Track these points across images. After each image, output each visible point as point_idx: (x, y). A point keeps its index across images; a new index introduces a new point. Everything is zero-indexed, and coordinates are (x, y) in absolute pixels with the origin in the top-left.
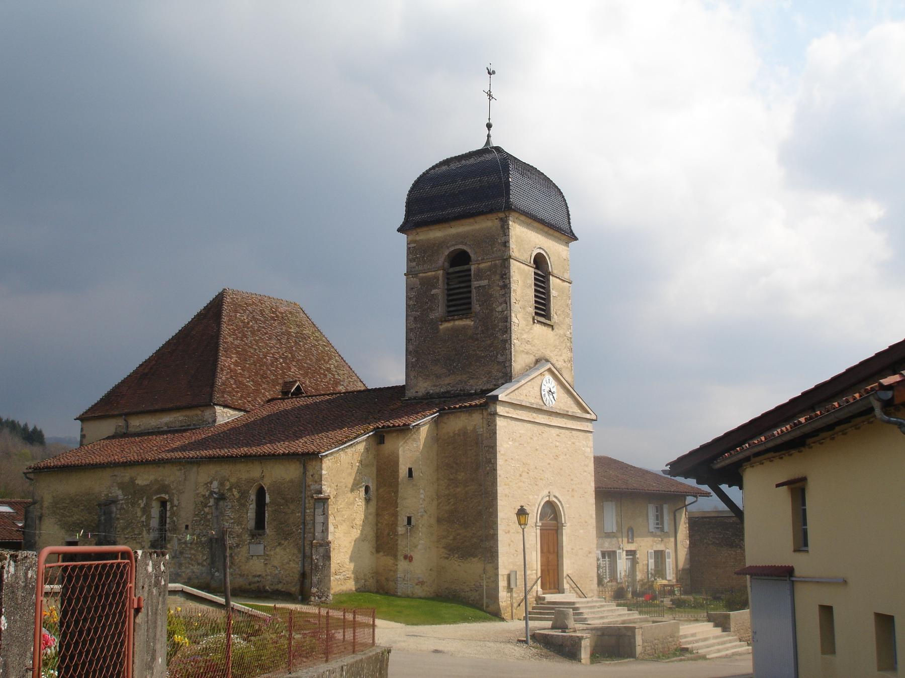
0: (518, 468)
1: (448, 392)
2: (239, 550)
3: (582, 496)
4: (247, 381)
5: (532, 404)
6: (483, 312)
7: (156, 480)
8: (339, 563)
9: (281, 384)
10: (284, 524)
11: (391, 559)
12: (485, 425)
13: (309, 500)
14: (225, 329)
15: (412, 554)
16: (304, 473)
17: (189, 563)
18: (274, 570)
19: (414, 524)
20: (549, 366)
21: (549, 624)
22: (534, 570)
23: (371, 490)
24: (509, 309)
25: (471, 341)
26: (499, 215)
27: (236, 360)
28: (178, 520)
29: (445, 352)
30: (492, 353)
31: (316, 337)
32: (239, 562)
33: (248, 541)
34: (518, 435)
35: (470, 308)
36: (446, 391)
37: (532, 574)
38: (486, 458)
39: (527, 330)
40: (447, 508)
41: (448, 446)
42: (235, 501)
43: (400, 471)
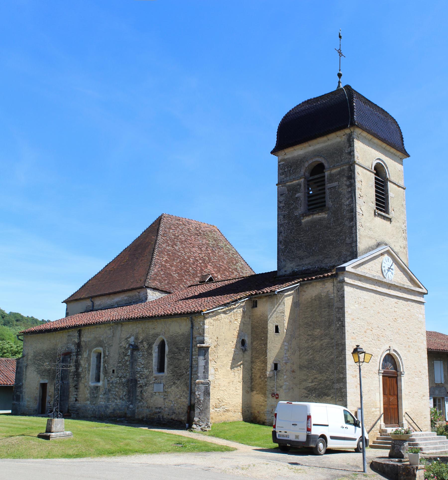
0: (363, 326)
1: (308, 269)
2: (146, 388)
3: (416, 351)
5: (374, 276)
6: (334, 207)
7: (95, 338)
8: (218, 399)
10: (177, 367)
11: (262, 397)
12: (335, 292)
13: (195, 349)
14: (160, 239)
15: (278, 392)
16: (192, 328)
19: (280, 370)
20: (389, 248)
21: (386, 453)
24: (354, 202)
25: (325, 229)
30: (342, 237)
31: (227, 248)
32: (147, 397)
33: (153, 381)
34: (363, 300)
35: (325, 206)
36: (307, 269)
37: (376, 411)
38: (337, 317)
39: (369, 220)
41: (307, 309)
42: (145, 351)
43: (269, 328)
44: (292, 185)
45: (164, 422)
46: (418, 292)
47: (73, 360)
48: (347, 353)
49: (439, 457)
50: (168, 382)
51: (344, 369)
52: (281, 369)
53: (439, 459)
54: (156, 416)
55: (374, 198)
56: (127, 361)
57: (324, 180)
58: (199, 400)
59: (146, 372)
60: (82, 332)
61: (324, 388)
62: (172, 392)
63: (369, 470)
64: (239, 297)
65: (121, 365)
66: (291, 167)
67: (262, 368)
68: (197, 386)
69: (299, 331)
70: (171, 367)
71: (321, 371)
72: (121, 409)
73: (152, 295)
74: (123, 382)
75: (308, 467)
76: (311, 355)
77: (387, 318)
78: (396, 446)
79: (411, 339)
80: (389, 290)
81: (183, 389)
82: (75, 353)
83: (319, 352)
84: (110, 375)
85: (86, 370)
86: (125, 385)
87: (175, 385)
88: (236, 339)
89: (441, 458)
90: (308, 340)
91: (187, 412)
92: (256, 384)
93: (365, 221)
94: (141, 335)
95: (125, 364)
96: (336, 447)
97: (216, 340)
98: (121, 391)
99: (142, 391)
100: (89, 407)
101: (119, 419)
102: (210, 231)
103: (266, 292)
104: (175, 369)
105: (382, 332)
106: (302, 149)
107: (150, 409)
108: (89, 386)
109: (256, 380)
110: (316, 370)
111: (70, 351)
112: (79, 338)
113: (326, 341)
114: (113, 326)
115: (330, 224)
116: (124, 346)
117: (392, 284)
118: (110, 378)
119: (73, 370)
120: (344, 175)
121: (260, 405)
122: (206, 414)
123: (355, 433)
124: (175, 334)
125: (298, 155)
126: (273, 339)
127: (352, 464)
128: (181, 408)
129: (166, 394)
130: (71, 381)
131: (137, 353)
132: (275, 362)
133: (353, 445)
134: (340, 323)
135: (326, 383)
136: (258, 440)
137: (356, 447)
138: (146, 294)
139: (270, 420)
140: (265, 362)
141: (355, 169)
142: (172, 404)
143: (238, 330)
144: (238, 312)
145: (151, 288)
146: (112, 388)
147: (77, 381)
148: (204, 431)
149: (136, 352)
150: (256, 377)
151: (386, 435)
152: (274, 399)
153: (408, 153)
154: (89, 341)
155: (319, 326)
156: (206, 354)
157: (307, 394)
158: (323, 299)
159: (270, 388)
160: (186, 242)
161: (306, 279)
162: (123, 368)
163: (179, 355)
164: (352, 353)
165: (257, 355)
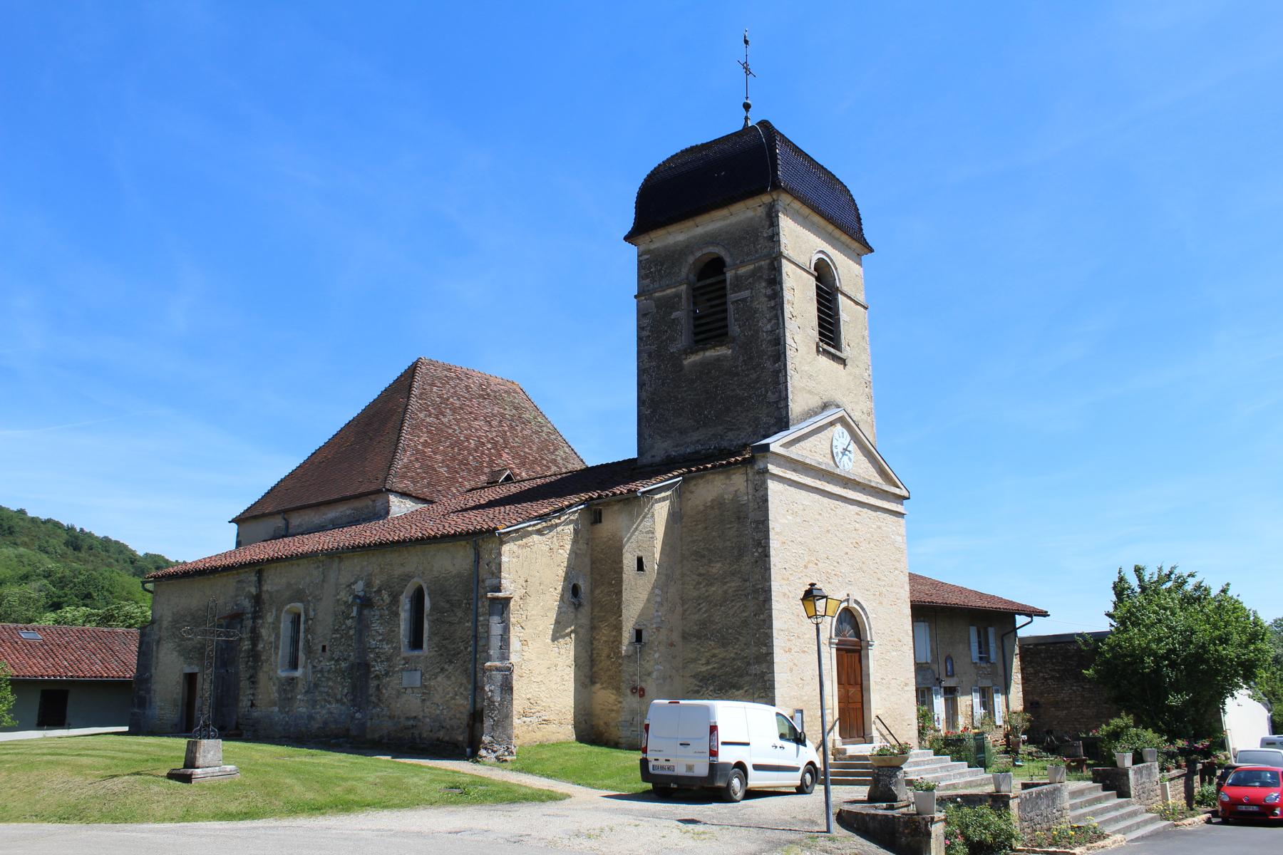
1: (697, 452)
2: (388, 679)
4: (440, 466)
5: (819, 463)
6: (744, 335)
9: (486, 474)
10: (447, 639)
11: (613, 694)
12: (751, 491)
13: (483, 602)
14: (414, 403)
15: (643, 685)
17: (326, 700)
18: (435, 710)
19: (647, 641)
20: (842, 413)
21: (862, 792)
22: (829, 709)
25: (727, 377)
26: (763, 200)
28: (313, 639)
29: (692, 397)
32: (388, 697)
33: (401, 666)
38: (753, 539)
39: (809, 360)
40: (696, 617)
41: (696, 525)
42: (385, 608)
43: (625, 561)
44: (663, 296)
46: (894, 494)
48: (773, 607)
49: (958, 796)
50: (431, 668)
51: (769, 637)
52: (649, 640)
53: (959, 799)
55: (815, 322)
56: (350, 628)
57: (724, 288)
58: (492, 702)
59: (386, 647)
60: (265, 574)
61: (730, 674)
62: (439, 686)
63: (836, 829)
64: (566, 503)
65: (338, 636)
66: (662, 265)
67: (611, 639)
69: (682, 568)
70: (436, 639)
71: (726, 641)
73: (399, 507)
75: (718, 828)
76: (706, 612)
77: (843, 542)
78: (881, 778)
79: (884, 580)
80: (845, 490)
81: (459, 681)
82: (250, 615)
83: (721, 606)
84: (318, 656)
85: (272, 647)
86: (346, 674)
89: (961, 796)
90: (699, 583)
91: (468, 725)
92: (601, 669)
93: (800, 362)
95: (346, 634)
96: (764, 785)
99: (379, 685)
100: (277, 718)
102: (506, 392)
103: (618, 492)
105: (835, 567)
106: (682, 232)
107: (396, 720)
108: (278, 678)
109: (601, 661)
110: (714, 641)
112: (257, 585)
113: (734, 584)
114: (323, 561)
115: (736, 367)
116: (345, 599)
117: (850, 479)
118: (316, 661)
119: (246, 647)
120: (761, 277)
121: (609, 710)
123: (797, 756)
125: (675, 242)
126: (633, 583)
127: (801, 817)
128: (456, 718)
129: (427, 692)
132: (638, 627)
133: (794, 779)
134: (760, 550)
135: (735, 665)
136: (611, 777)
137: (798, 783)
139: (629, 737)
140: (618, 627)
141: (781, 266)
144: (565, 531)
145: (396, 492)
147: (254, 668)
148: (503, 761)
150: (601, 656)
151: (845, 760)
152: (637, 698)
153: (870, 244)
154: (277, 591)
155: (720, 557)
157: (698, 686)
158: (728, 506)
159: (628, 677)
160: (462, 409)
161: (693, 469)
164: (801, 599)
165: (604, 614)
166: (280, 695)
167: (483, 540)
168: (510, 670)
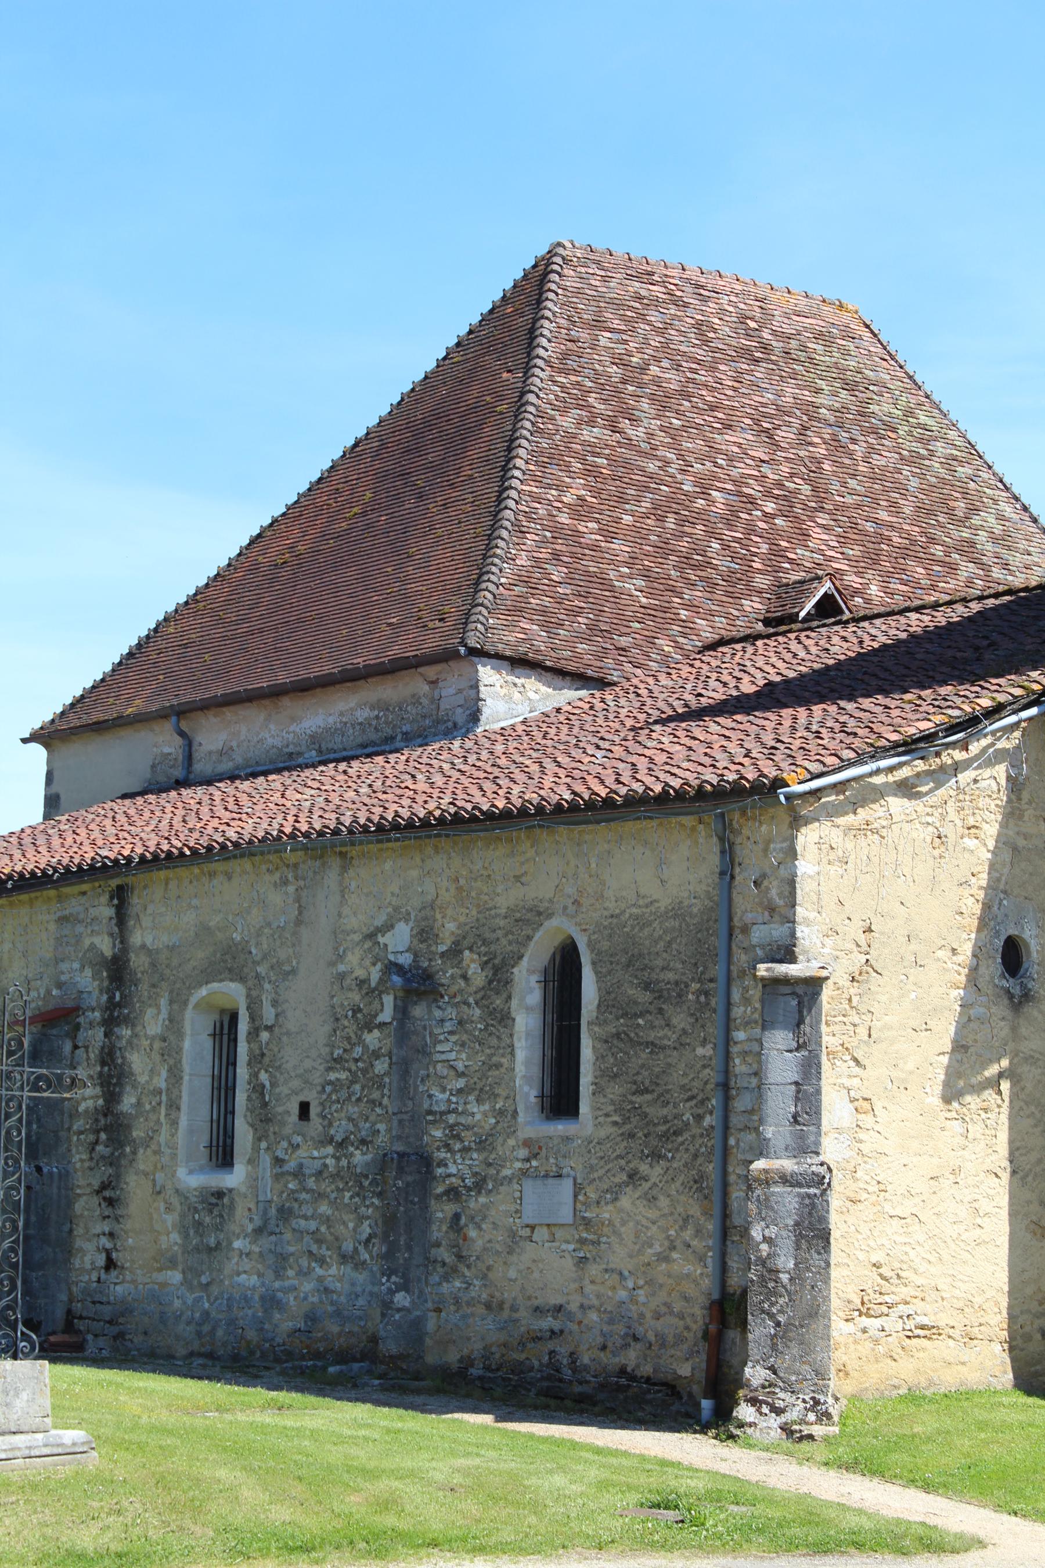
2: (482, 1200)
10: (647, 1091)
13: (746, 989)
16: (727, 873)
23: (1034, 955)
27: (580, 498)
32: (485, 1249)
33: (518, 1165)
42: (471, 1000)
45: (578, 1389)
47: (86, 1047)
50: (601, 1172)
54: (537, 1356)
58: (770, 1271)
59: (479, 1113)
60: (135, 900)
62: (624, 1223)
64: (986, 703)
65: (343, 1076)
68: (758, 1192)
70: (615, 1091)
72: (346, 1313)
74: (358, 1170)
81: (680, 1209)
82: (97, 1014)
84: (287, 1130)
85: (159, 1104)
86: (366, 1183)
87: (635, 1187)
88: (973, 936)
91: (706, 1335)
94: (449, 912)
95: (364, 1071)
97: (862, 939)
98: (345, 1217)
99: (457, 1217)
100: (177, 1303)
101: (338, 1368)
102: (819, 336)
104: (638, 1099)
107: (506, 1314)
108: (177, 1191)
111: (70, 1004)
112: (116, 929)
114: (296, 866)
116: (360, 973)
118: (285, 1144)
119: (90, 1103)
122: (807, 1348)
124: (634, 910)
128: (671, 1313)
129: (591, 1237)
130: (82, 1161)
131: (430, 1012)
138: (472, 693)
142: (625, 1288)
143: (981, 888)
144: (982, 784)
145: (498, 656)
146: (296, 1200)
147: (112, 1161)
148: (801, 1439)
149: (424, 1004)
154: (172, 948)
156: (807, 1020)
160: (688, 397)
162: (354, 1093)
163: (657, 1023)
166: (186, 1236)
167: (744, 813)
168: (821, 1182)
